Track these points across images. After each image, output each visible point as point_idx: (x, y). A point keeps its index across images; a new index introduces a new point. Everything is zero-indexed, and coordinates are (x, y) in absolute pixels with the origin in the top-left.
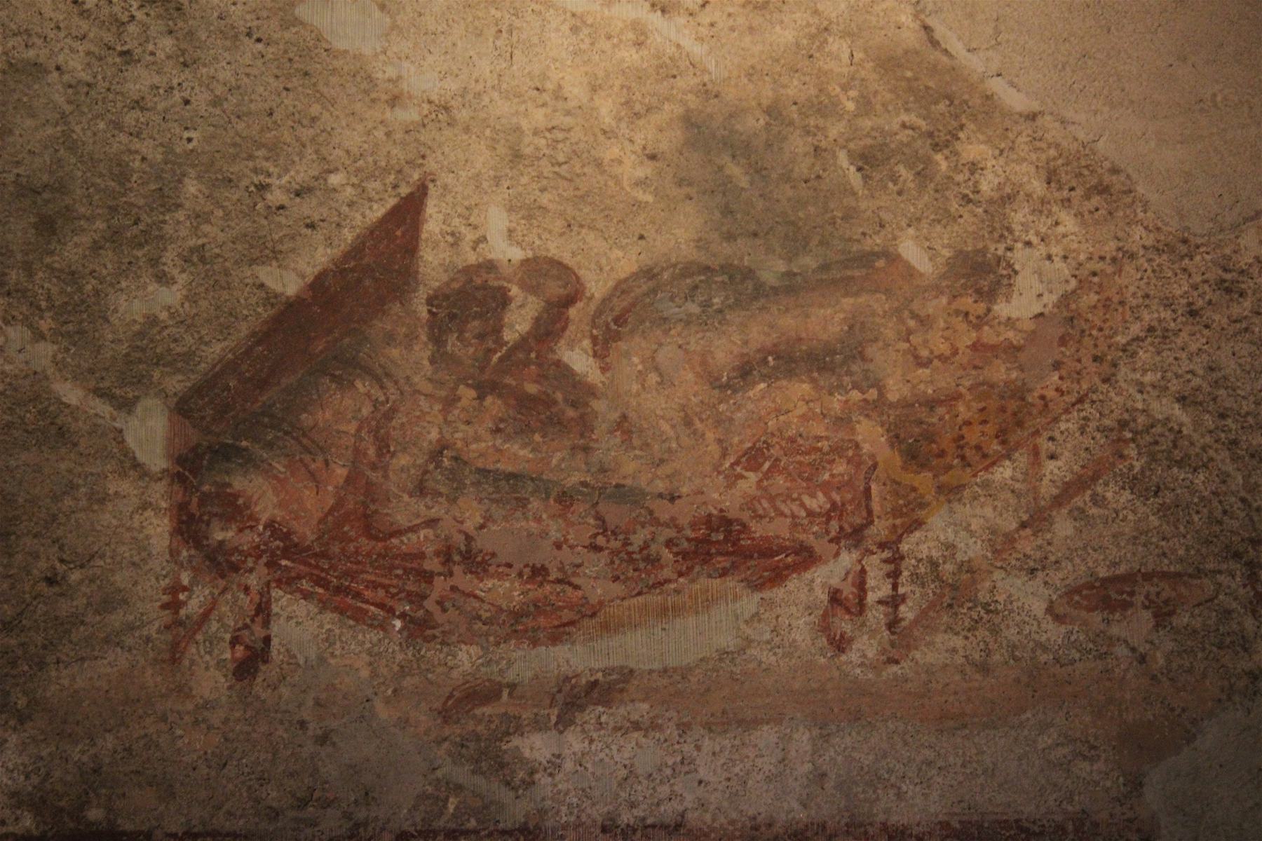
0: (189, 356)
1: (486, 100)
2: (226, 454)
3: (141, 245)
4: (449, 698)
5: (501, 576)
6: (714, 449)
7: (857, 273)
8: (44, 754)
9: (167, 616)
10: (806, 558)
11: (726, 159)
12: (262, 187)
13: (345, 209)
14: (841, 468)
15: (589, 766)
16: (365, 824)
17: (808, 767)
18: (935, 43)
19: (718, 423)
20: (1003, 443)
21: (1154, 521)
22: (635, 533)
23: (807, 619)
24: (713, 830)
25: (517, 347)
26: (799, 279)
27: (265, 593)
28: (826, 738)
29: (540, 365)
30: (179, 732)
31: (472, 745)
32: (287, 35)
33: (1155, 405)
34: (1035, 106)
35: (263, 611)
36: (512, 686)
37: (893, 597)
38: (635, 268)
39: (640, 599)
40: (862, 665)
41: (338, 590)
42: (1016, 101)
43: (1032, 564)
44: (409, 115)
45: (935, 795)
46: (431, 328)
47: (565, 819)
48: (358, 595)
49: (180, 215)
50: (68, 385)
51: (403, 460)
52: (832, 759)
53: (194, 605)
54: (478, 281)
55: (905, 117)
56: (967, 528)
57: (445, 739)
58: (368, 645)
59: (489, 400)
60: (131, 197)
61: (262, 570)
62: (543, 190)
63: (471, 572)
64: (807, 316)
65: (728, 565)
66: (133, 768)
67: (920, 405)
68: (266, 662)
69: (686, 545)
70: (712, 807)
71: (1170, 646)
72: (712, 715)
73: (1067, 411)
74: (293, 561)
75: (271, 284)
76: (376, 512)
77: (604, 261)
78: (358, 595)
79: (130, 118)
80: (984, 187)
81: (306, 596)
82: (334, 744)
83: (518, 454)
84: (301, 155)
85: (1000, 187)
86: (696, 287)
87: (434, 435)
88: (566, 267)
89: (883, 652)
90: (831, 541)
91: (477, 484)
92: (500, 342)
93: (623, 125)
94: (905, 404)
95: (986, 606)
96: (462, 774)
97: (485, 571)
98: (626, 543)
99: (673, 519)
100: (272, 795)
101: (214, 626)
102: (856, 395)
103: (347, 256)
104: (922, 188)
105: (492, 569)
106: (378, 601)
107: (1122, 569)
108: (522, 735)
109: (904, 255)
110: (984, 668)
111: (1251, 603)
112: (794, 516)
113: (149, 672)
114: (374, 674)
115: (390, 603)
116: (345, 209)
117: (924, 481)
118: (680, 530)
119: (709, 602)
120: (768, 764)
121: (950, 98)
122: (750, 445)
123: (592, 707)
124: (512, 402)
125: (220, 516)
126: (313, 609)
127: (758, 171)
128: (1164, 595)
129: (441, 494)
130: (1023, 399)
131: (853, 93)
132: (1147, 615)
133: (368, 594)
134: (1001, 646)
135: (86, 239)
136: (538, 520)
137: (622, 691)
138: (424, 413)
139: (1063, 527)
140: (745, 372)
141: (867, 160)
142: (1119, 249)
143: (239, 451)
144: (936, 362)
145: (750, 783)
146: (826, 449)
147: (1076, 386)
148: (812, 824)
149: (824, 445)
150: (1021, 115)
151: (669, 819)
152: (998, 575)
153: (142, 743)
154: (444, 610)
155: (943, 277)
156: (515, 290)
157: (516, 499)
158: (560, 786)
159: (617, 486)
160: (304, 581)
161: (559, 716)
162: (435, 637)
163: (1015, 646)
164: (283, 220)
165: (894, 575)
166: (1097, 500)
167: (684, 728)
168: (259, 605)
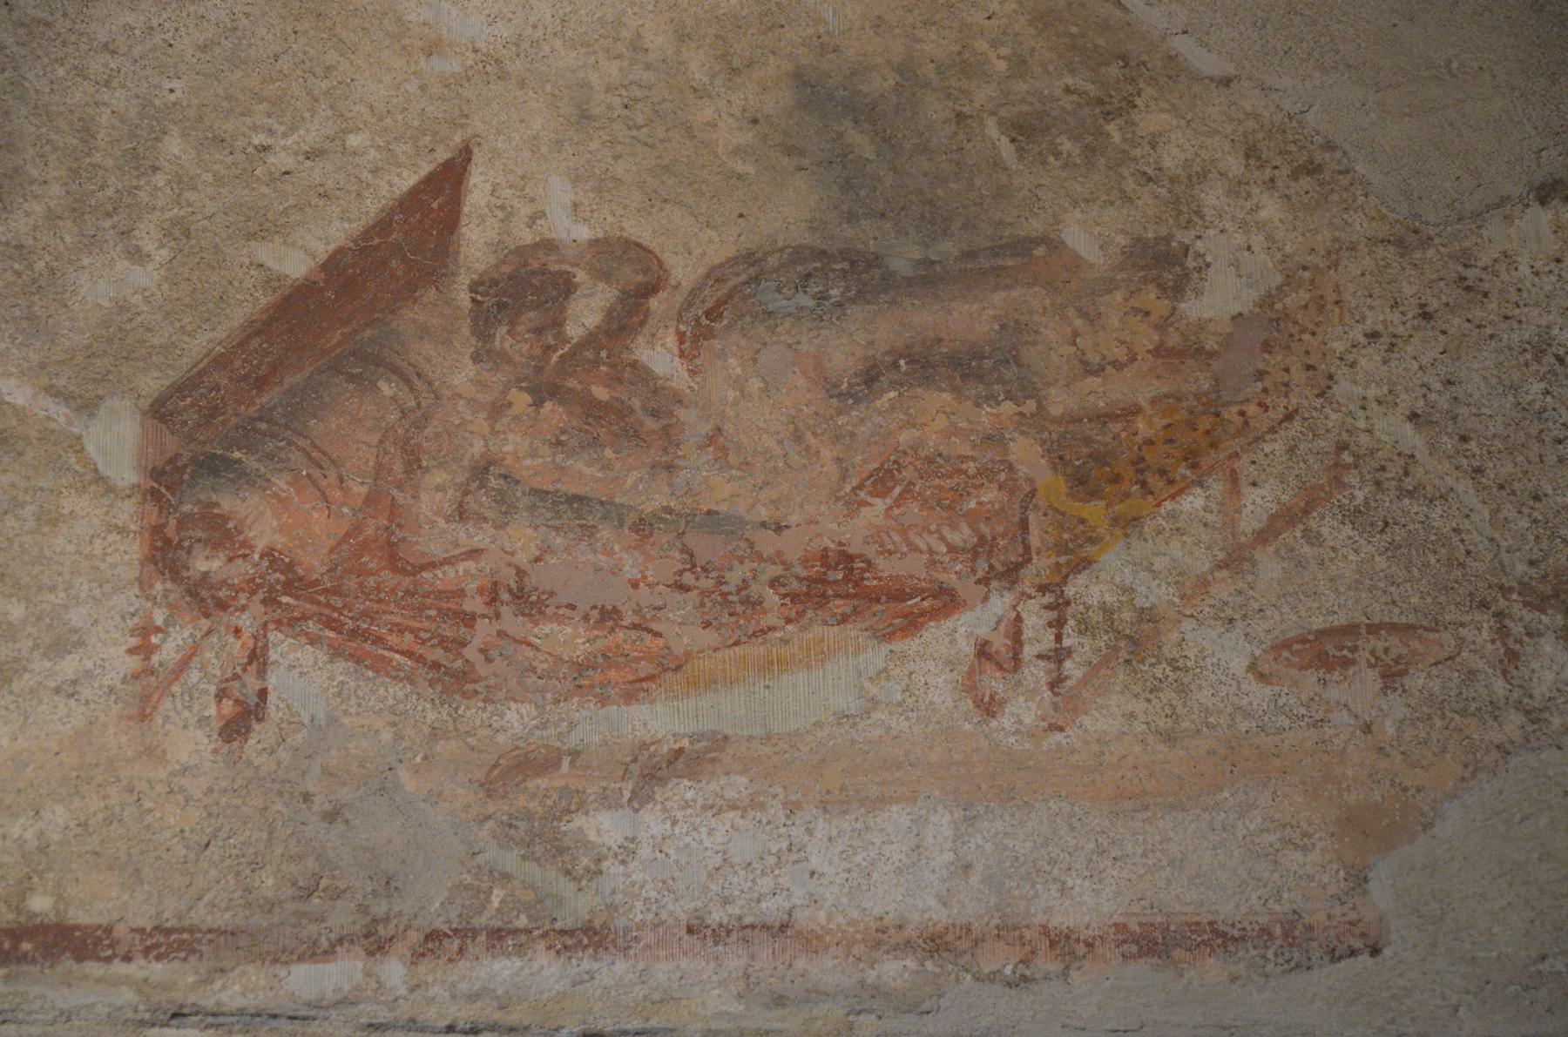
2: (213, 467)
3: (109, 215)
4: (495, 766)
6: (832, 469)
9: (134, 663)
10: (947, 601)
12: (265, 149)
13: (366, 176)
14: (990, 495)
15: (671, 852)
16: (387, 919)
19: (837, 438)
20: (1194, 466)
21: (1381, 562)
22: (731, 569)
23: (949, 676)
25: (584, 343)
26: (938, 268)
27: (260, 636)
28: (971, 820)
29: (613, 366)
30: (148, 804)
31: (523, 825)
33: (1379, 425)
34: (1231, 70)
35: (257, 658)
36: (575, 754)
37: (1056, 650)
38: (732, 253)
40: (1017, 732)
41: (354, 633)
42: (1206, 62)
43: (1229, 612)
44: (453, 66)
46: (475, 320)
47: (640, 917)
48: (379, 640)
49: (160, 179)
50: (13, 381)
52: (978, 846)
53: (169, 650)
54: (535, 265)
55: (1069, 80)
56: (1149, 569)
57: (489, 817)
58: (391, 702)
59: (548, 406)
60: (98, 158)
61: (257, 608)
62: (617, 157)
63: (523, 615)
64: (949, 312)
65: (848, 610)
66: (88, 848)
67: (1090, 420)
68: (259, 720)
69: (795, 585)
70: (827, 904)
71: (1401, 712)
72: (828, 792)
73: (1272, 430)
74: (297, 598)
75: (270, 263)
76: (404, 539)
77: (693, 244)
78: (379, 640)
79: (99, 64)
80: (1167, 163)
81: (314, 641)
82: (347, 822)
83: (584, 473)
84: (313, 112)
85: (1187, 164)
86: (809, 275)
87: (478, 448)
88: (650, 252)
90: (978, 582)
92: (562, 338)
93: (718, 82)
95: (1172, 662)
96: (510, 860)
97: (541, 612)
98: (721, 582)
99: (779, 553)
100: (267, 882)
101: (194, 676)
102: (1008, 408)
103: (367, 234)
105: (550, 611)
106: (405, 647)
107: (1341, 620)
108: (587, 814)
109: (1069, 242)
110: (1169, 738)
111: (1501, 662)
112: (931, 552)
113: (112, 730)
114: (398, 737)
115: (419, 649)
116: (366, 176)
117: (1094, 511)
118: (788, 566)
121: (1124, 58)
122: (876, 465)
123: (676, 781)
125: (207, 542)
126: (322, 657)
128: (1394, 652)
129: (485, 520)
130: (1217, 415)
131: (1005, 51)
132: (1373, 675)
133: (392, 639)
134: (1191, 711)
135: (38, 208)
136: (610, 553)
138: (464, 423)
139: (1270, 567)
140: (870, 377)
141: (1023, 131)
142: (1335, 240)
143: (229, 464)
144: (1109, 369)
145: (875, 875)
146: (972, 471)
147: (1283, 402)
148: (954, 926)
149: (971, 467)
150: (1212, 79)
152: (1188, 625)
153: (100, 816)
154: (489, 660)
156: (581, 276)
157: (581, 526)
158: (634, 877)
159: (709, 513)
160: (311, 623)
161: (633, 792)
162: (477, 692)
164: (289, 188)
165: (1058, 624)
166: (1312, 537)
167: (792, 809)
168: (254, 650)
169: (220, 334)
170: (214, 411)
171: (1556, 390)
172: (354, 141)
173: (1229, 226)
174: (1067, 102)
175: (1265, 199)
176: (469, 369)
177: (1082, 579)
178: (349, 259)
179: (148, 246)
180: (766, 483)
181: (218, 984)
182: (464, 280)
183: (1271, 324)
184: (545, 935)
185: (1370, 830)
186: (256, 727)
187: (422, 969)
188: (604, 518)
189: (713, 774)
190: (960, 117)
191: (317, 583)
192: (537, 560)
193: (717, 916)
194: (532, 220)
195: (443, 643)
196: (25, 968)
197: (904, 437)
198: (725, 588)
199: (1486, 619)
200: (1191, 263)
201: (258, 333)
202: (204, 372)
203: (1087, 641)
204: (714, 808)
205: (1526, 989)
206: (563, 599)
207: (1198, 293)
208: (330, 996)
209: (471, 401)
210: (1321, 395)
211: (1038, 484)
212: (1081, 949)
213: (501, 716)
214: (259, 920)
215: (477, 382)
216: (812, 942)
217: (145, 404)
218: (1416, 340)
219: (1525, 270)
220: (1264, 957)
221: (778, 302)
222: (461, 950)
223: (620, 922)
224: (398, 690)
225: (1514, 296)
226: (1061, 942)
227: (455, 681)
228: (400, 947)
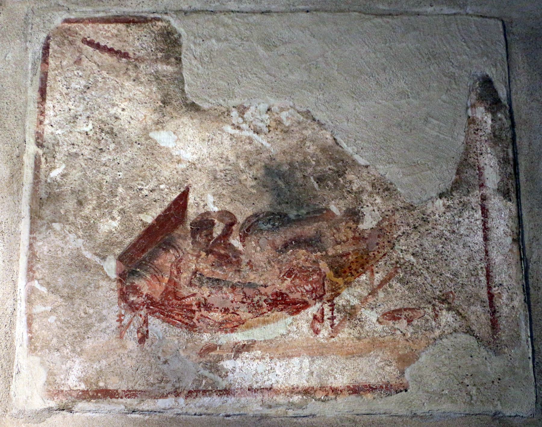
0: (121, 242)
2: (133, 273)
3: (106, 208)
4: (202, 349)
5: (215, 311)
6: (278, 271)
7: (318, 215)
8: (86, 366)
9: (118, 324)
10: (306, 305)
11: (277, 179)
12: (141, 189)
16: (179, 388)
17: (308, 370)
18: (337, 144)
20: (363, 268)
21: (407, 292)
23: (307, 324)
24: (281, 390)
25: (217, 239)
28: (313, 361)
29: (224, 244)
30: (123, 360)
32: (147, 142)
33: (406, 256)
34: (368, 163)
35: (146, 322)
36: (220, 346)
38: (252, 214)
39: (257, 318)
40: (323, 338)
41: (167, 316)
42: (362, 161)
43: (372, 306)
44: (183, 166)
45: (345, 378)
48: (173, 317)
49: (117, 199)
50: (87, 252)
51: (185, 275)
53: (126, 321)
54: (205, 218)
55: (330, 167)
56: (353, 295)
58: (177, 333)
59: (210, 255)
60: (104, 193)
61: (145, 310)
62: (223, 189)
64: (304, 229)
65: (283, 307)
68: (147, 338)
69: (270, 301)
70: (280, 383)
71: (412, 330)
73: (381, 258)
75: (144, 220)
77: (242, 211)
78: (173, 317)
79: (102, 169)
80: (354, 188)
81: (159, 318)
83: (219, 273)
85: (359, 188)
86: (270, 219)
87: (194, 267)
89: (329, 334)
90: (313, 299)
91: (207, 282)
92: (212, 238)
93: (247, 168)
94: (334, 256)
95: (359, 319)
100: (151, 379)
101: (132, 327)
102: (319, 254)
103: (165, 211)
104: (336, 188)
105: (213, 309)
107: (398, 308)
110: (359, 339)
112: (302, 292)
113: (114, 341)
114: (179, 342)
115: (183, 320)
116: (165, 196)
117: (340, 280)
118: (268, 296)
119: (277, 319)
120: (296, 369)
124: (217, 256)
125: (132, 293)
127: (287, 183)
128: (410, 315)
129: (196, 286)
130: (368, 254)
133: (176, 317)
135: (91, 207)
136: (226, 294)
137: (253, 347)
138: (190, 260)
139: (381, 294)
140: (286, 246)
141: (320, 180)
142: (393, 208)
143: (137, 272)
144: (342, 243)
146: (311, 270)
147: (383, 250)
149: (311, 269)
150: (363, 166)
151: (268, 387)
152: (363, 310)
153: (113, 363)
154: (199, 322)
155: (344, 216)
156: (216, 221)
159: (249, 283)
163: (368, 332)
164: (147, 200)
165: (332, 310)
166: (391, 286)
167: (271, 358)
169: (133, 238)
171: (445, 247)
172: (162, 187)
173: (369, 205)
174: (330, 172)
175: (377, 198)
177: (337, 298)
178: (161, 218)
179: (116, 216)
180: (262, 275)
181: (142, 404)
182: (189, 223)
183: (379, 230)
184: (215, 391)
185: (405, 360)
186: (146, 340)
187: (188, 400)
188: (224, 285)
191: (158, 303)
192: (209, 296)
193: (255, 386)
194: (204, 206)
195: (188, 318)
197: (295, 262)
198: (253, 302)
199: (430, 306)
200: (360, 215)
201: (141, 238)
204: (253, 359)
205: (439, 398)
207: (362, 223)
208: (167, 407)
209: (192, 255)
210: (392, 249)
211: (327, 274)
212: (339, 392)
214: (150, 388)
215: (192, 250)
216: (277, 392)
218: (413, 234)
219: (437, 216)
220: (381, 393)
221: (264, 227)
222: (196, 396)
223: (233, 388)
224: (179, 330)
225: (435, 223)
226: (335, 391)
227: (191, 328)
228: (183, 395)
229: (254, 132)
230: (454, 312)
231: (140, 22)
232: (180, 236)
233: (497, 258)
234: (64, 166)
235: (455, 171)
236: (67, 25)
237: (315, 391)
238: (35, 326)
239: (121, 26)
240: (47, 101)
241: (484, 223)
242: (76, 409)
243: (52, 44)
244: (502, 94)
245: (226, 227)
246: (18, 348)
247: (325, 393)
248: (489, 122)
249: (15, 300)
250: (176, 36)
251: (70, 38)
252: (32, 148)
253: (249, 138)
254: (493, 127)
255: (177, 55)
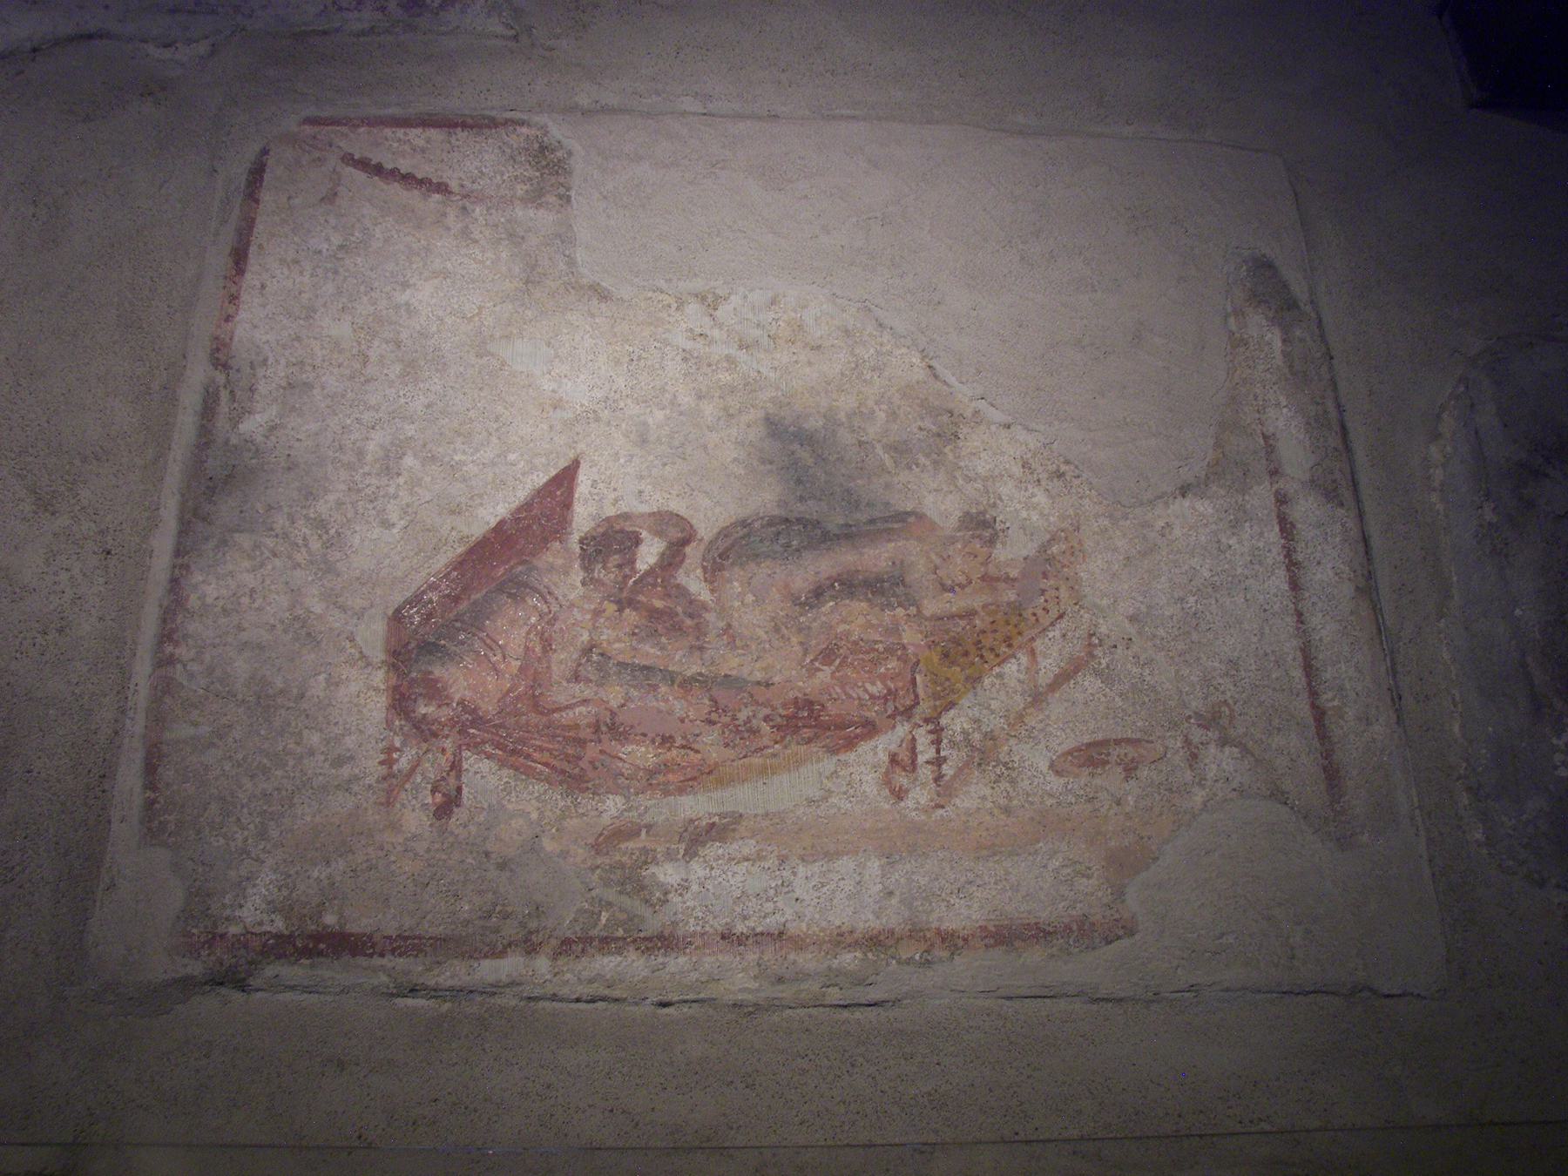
1: (622, 404)
2: (429, 649)
6: (797, 648)
9: (383, 770)
10: (870, 729)
11: (796, 446)
18: (936, 377)
20: (1010, 646)
25: (648, 573)
34: (1010, 419)
35: (456, 767)
36: (649, 827)
48: (528, 756)
49: (401, 480)
53: (403, 763)
54: (617, 527)
73: (1052, 624)
78: (528, 756)
79: (367, 417)
80: (980, 470)
81: (489, 756)
83: (649, 653)
86: (779, 533)
87: (585, 637)
95: (1005, 764)
96: (611, 894)
98: (734, 718)
102: (900, 611)
103: (519, 510)
107: (1100, 736)
110: (1007, 811)
119: (800, 762)
120: (848, 885)
121: (951, 413)
126: (494, 766)
128: (1130, 756)
131: (884, 407)
132: (1120, 769)
133: (536, 755)
139: (1056, 707)
140: (818, 593)
149: (880, 647)
152: (1012, 742)
156: (644, 534)
165: (937, 742)
167: (783, 860)
170: (430, 615)
172: (512, 457)
174: (921, 435)
176: (581, 590)
177: (952, 712)
179: (394, 517)
181: (436, 972)
182: (576, 537)
183: (1045, 564)
184: (635, 941)
189: (734, 839)
190: (861, 444)
191: (489, 721)
193: (740, 928)
194: (616, 501)
196: (322, 959)
197: (841, 628)
200: (998, 526)
202: (424, 592)
203: (955, 753)
206: (639, 730)
207: (1004, 544)
212: (960, 943)
213: (604, 802)
216: (799, 943)
217: (390, 612)
223: (680, 933)
224: (539, 788)
226: (952, 941)
227: (574, 781)
229: (740, 347)
230: (1235, 750)
231: (480, 127)
232: (551, 568)
233: (1324, 628)
234: (274, 411)
235: (1211, 441)
236: (308, 130)
237: (899, 940)
238: (167, 773)
239: (434, 133)
240: (248, 276)
241: (1289, 553)
242: (254, 982)
243: (271, 161)
244: (1299, 290)
245: (668, 548)
246: (115, 826)
247: (923, 946)
248: (1278, 344)
249: (123, 711)
250: (559, 154)
251: (317, 154)
252: (198, 373)
253: (728, 358)
254: (1285, 354)
255: (562, 190)
